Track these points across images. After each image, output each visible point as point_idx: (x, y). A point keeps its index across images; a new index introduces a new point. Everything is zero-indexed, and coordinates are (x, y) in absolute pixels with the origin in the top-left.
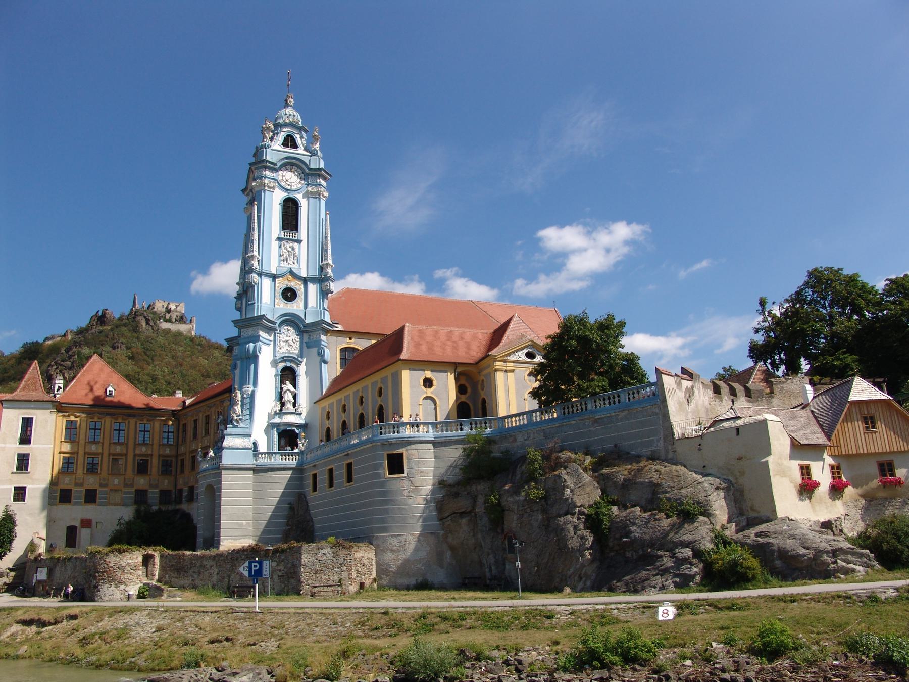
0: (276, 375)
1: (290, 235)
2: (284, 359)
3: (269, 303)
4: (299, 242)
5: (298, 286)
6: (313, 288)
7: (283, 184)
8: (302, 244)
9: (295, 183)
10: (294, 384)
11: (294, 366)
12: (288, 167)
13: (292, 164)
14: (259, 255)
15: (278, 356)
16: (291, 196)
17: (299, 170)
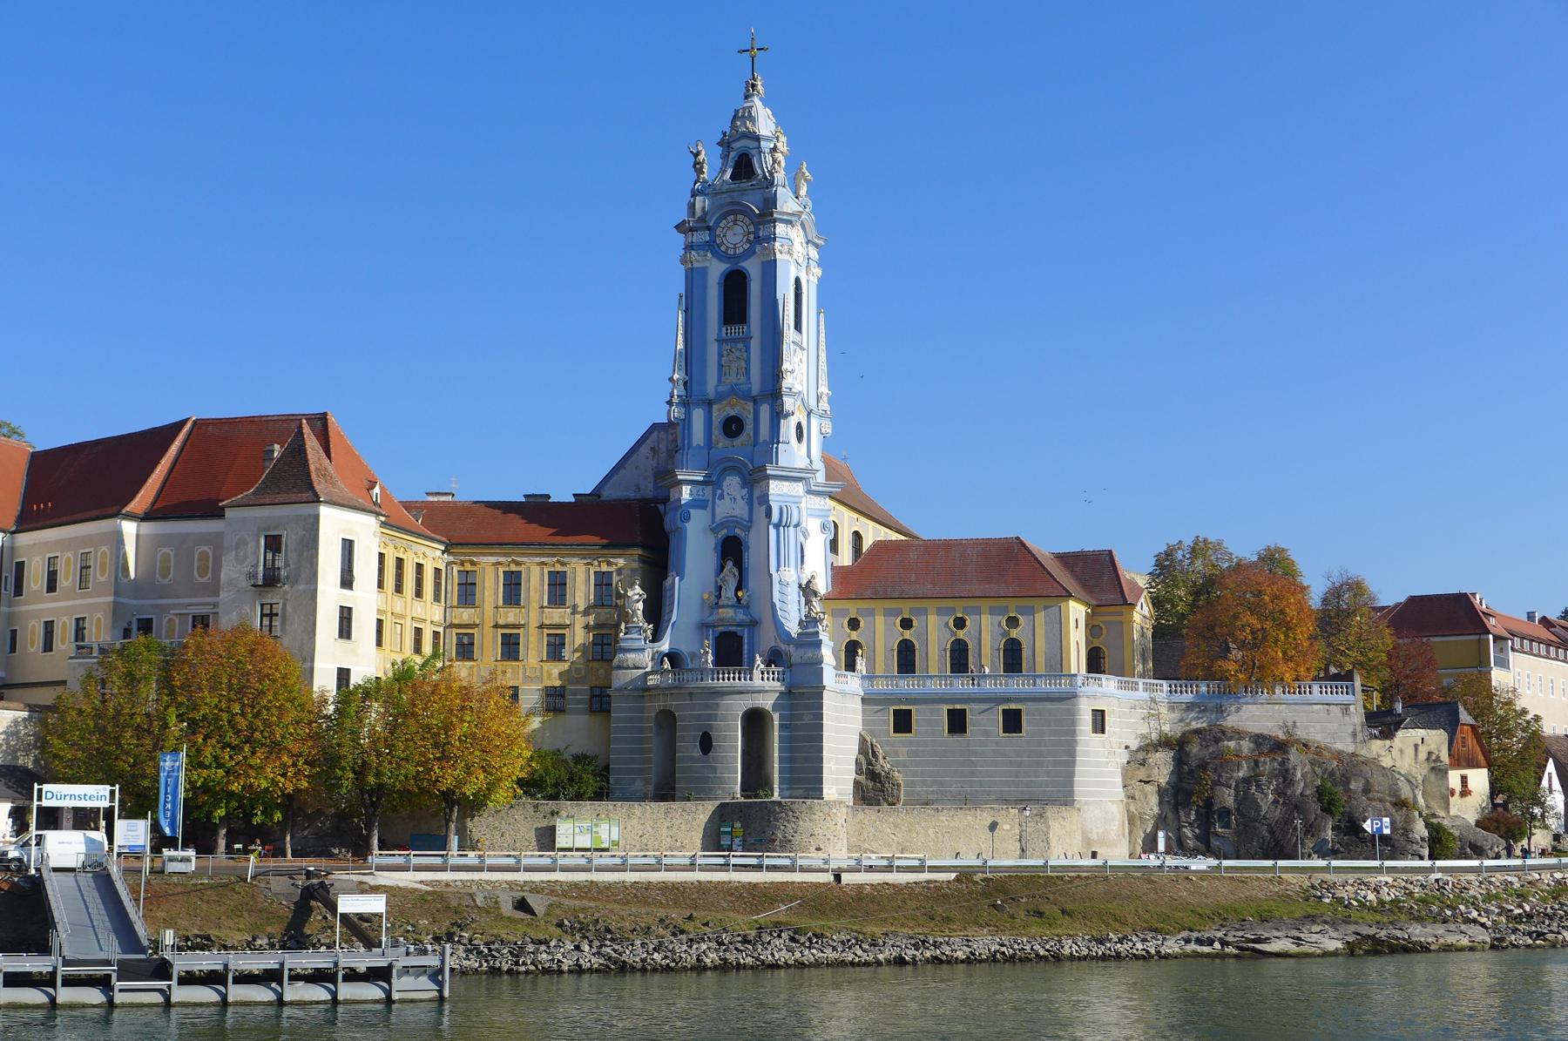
0: (715, 549)
1: (736, 330)
2: (723, 525)
3: (702, 445)
4: (746, 340)
5: (745, 410)
6: (765, 410)
7: (723, 248)
8: (752, 342)
9: (742, 243)
10: (739, 564)
11: (738, 531)
12: (731, 218)
13: (735, 213)
14: (686, 374)
15: (718, 519)
16: (735, 268)
17: (746, 219)
